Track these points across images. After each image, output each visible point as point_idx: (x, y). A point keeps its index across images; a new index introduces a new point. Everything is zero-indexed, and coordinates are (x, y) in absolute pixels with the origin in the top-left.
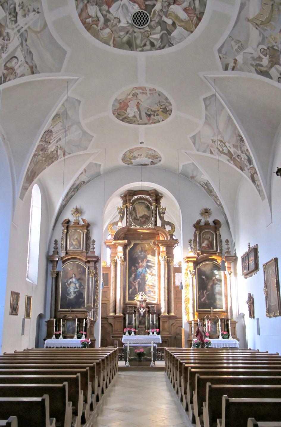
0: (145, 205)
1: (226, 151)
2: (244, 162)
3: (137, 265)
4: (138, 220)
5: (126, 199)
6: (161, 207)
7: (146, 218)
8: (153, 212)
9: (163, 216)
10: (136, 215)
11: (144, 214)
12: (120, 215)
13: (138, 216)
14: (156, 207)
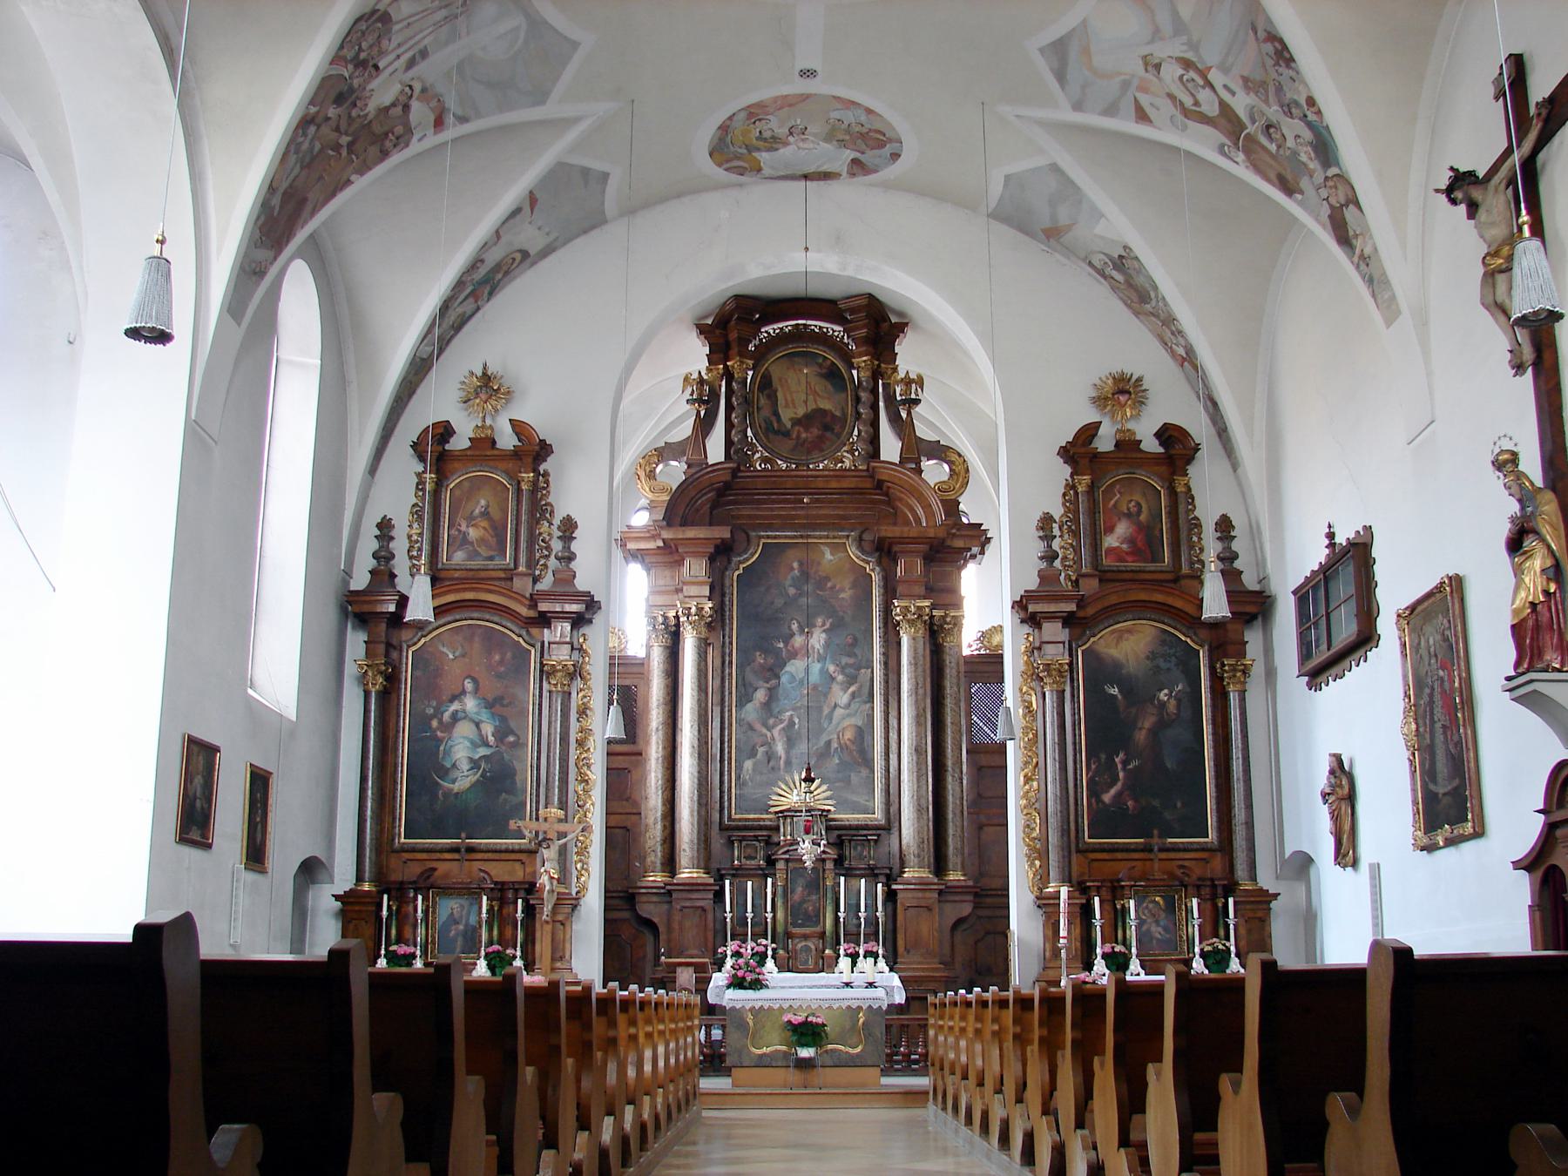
0: (820, 366)
1: (1212, 109)
2: (1295, 153)
3: (781, 645)
4: (787, 434)
5: (726, 336)
6: (902, 375)
7: (826, 428)
8: (858, 400)
9: (909, 414)
10: (776, 414)
11: (814, 407)
12: (698, 412)
13: (786, 415)
14: (876, 374)
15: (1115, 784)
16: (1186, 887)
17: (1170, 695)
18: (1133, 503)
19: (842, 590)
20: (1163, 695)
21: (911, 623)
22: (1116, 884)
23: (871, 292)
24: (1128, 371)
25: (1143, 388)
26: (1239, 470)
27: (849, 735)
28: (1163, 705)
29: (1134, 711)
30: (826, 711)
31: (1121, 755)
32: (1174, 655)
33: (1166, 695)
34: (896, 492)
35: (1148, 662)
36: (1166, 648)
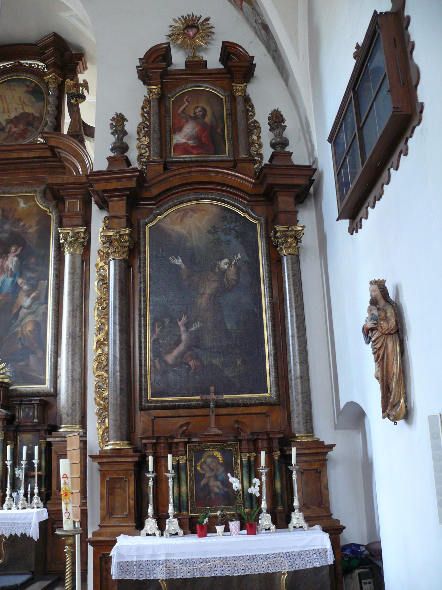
0: (28, 86)
7: (29, 124)
11: (22, 111)
15: (178, 345)
16: (240, 441)
17: (230, 264)
18: (199, 109)
19: (30, 227)
20: (224, 264)
21: (71, 244)
22: (170, 441)
24: (197, 14)
25: (210, 26)
26: (290, 81)
27: (29, 328)
28: (224, 273)
31: (184, 319)
32: (234, 229)
34: (64, 154)
35: (210, 236)
36: (226, 223)
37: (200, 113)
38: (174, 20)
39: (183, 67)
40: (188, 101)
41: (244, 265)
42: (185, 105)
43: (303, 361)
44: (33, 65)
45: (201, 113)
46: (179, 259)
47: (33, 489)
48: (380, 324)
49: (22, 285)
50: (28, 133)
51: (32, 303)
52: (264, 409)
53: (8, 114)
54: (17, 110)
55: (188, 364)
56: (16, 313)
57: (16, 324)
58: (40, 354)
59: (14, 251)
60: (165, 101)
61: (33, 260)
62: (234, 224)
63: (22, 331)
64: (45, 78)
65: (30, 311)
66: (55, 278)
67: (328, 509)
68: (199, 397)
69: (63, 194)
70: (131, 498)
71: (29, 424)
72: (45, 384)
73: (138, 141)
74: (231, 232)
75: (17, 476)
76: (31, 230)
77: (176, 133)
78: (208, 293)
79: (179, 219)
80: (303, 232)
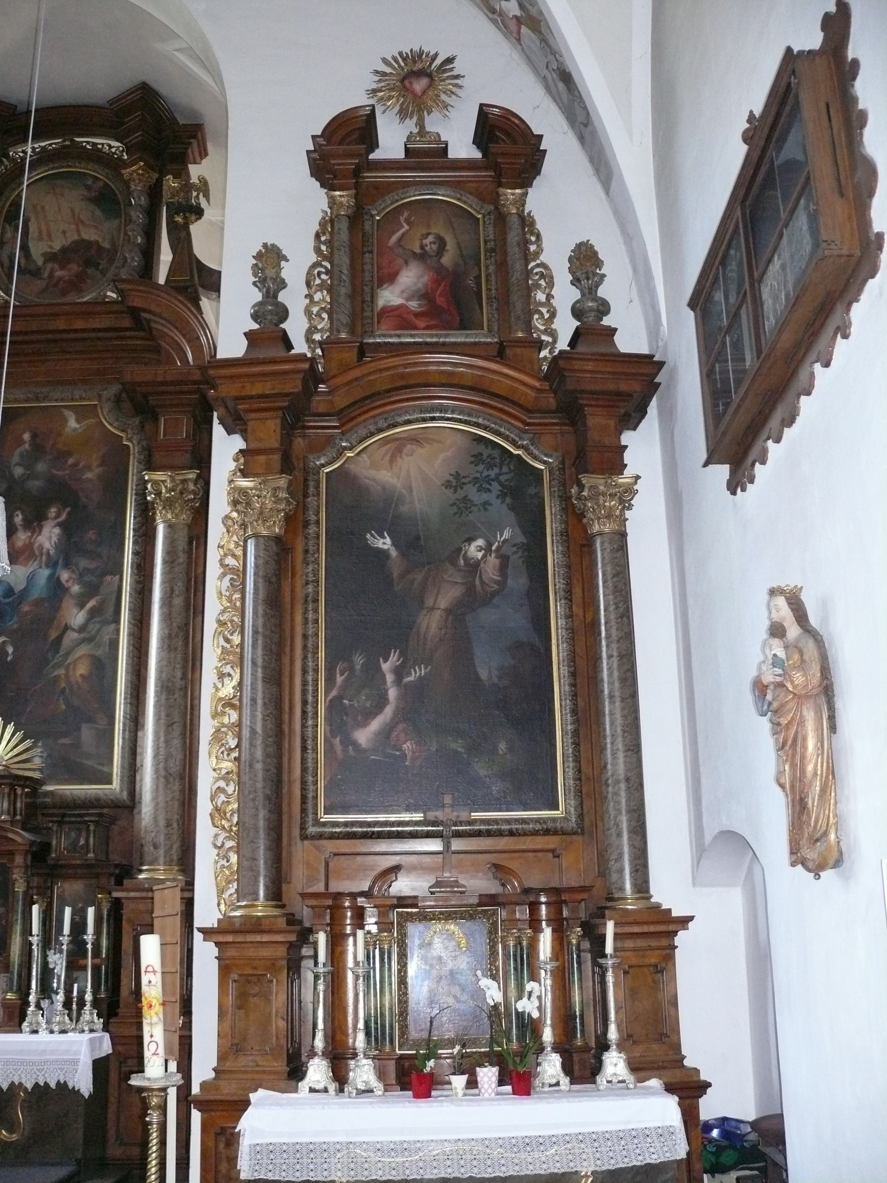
0: (89, 188)
7: (88, 263)
11: (76, 237)
13: (37, 250)
17: (488, 549)
18: (431, 238)
19: (89, 468)
20: (474, 550)
21: (169, 504)
23: (144, 78)
24: (430, 48)
25: (455, 73)
27: (82, 669)
28: (474, 567)
29: (419, 577)
30: (53, 635)
32: (496, 479)
33: (480, 549)
34: (158, 326)
35: (449, 492)
36: (481, 467)
37: (433, 246)
38: (385, 61)
39: (400, 154)
40: (408, 222)
41: (515, 553)
42: (403, 230)
43: (632, 748)
44: (100, 146)
45: (435, 247)
46: (384, 537)
47: (82, 993)
48: (790, 676)
49: (70, 584)
50: (89, 281)
51: (88, 621)
52: (551, 842)
53: (50, 243)
54: (68, 235)
55: (400, 750)
56: (58, 637)
57: (55, 661)
58: (102, 722)
59: (53, 515)
60: (363, 222)
61: (91, 535)
62: (496, 470)
63: (67, 676)
64: (123, 171)
65: (82, 635)
66: (135, 571)
67: (676, 1047)
68: (418, 816)
69: (155, 403)
70: (280, 1015)
71: (78, 862)
72: (111, 783)
73: (308, 301)
74: (491, 485)
75: (51, 966)
76: (89, 475)
77: (385, 286)
78: (442, 607)
79: (387, 458)
80: (636, 487)
